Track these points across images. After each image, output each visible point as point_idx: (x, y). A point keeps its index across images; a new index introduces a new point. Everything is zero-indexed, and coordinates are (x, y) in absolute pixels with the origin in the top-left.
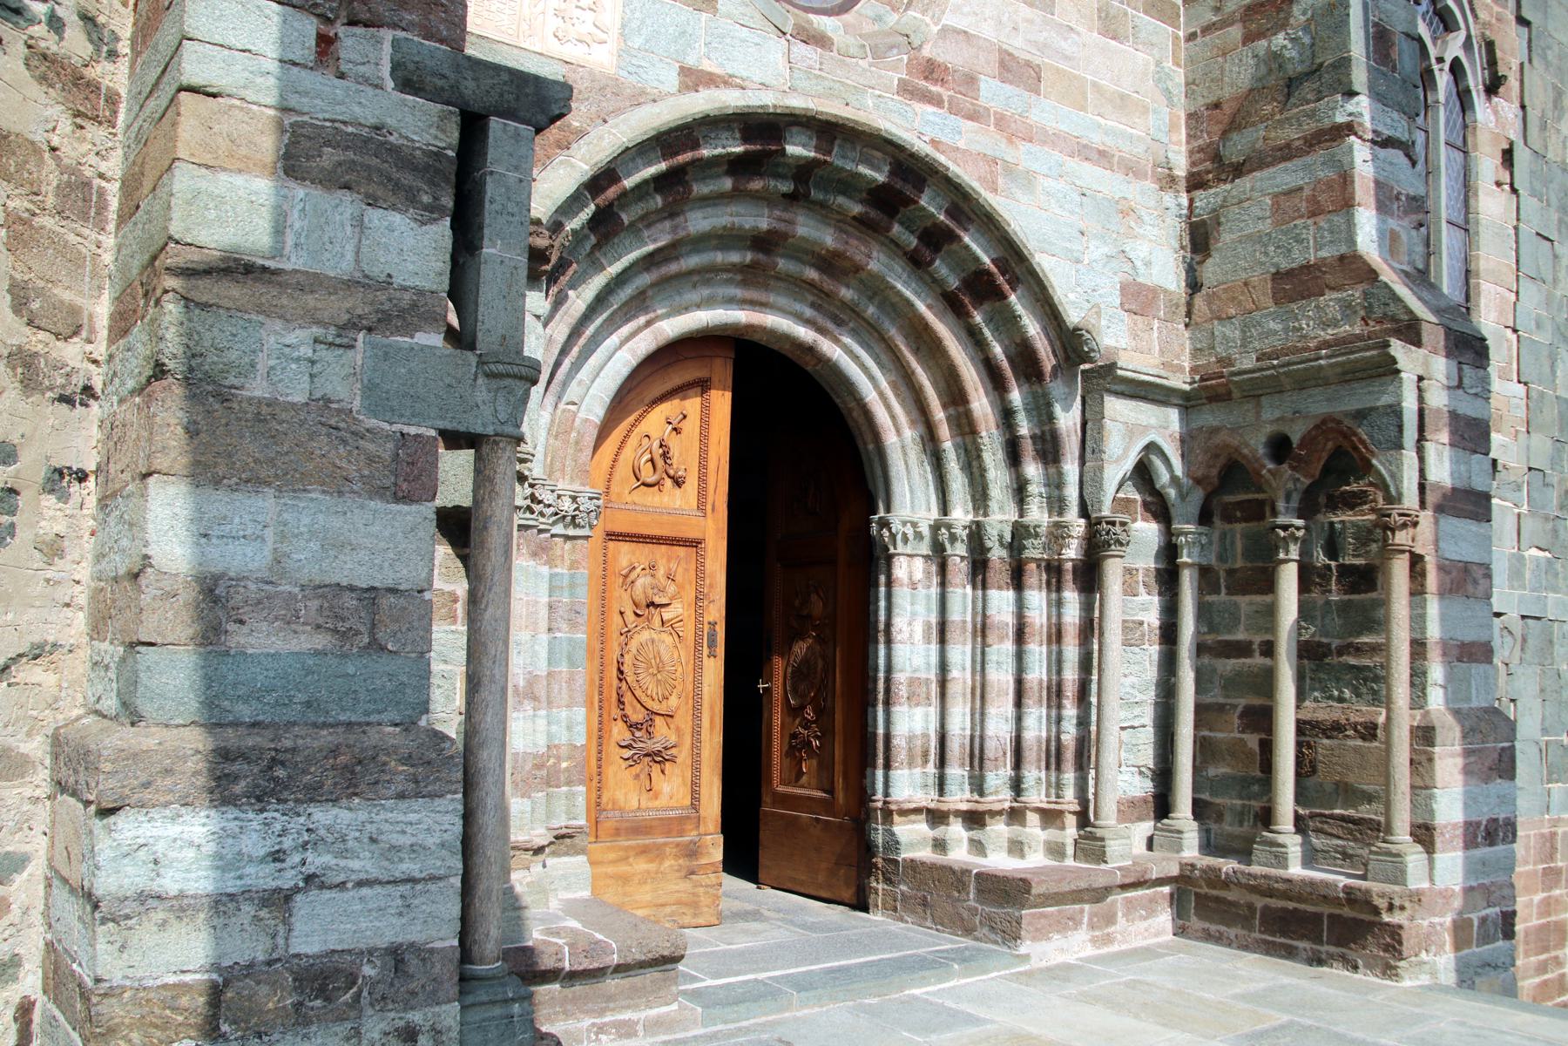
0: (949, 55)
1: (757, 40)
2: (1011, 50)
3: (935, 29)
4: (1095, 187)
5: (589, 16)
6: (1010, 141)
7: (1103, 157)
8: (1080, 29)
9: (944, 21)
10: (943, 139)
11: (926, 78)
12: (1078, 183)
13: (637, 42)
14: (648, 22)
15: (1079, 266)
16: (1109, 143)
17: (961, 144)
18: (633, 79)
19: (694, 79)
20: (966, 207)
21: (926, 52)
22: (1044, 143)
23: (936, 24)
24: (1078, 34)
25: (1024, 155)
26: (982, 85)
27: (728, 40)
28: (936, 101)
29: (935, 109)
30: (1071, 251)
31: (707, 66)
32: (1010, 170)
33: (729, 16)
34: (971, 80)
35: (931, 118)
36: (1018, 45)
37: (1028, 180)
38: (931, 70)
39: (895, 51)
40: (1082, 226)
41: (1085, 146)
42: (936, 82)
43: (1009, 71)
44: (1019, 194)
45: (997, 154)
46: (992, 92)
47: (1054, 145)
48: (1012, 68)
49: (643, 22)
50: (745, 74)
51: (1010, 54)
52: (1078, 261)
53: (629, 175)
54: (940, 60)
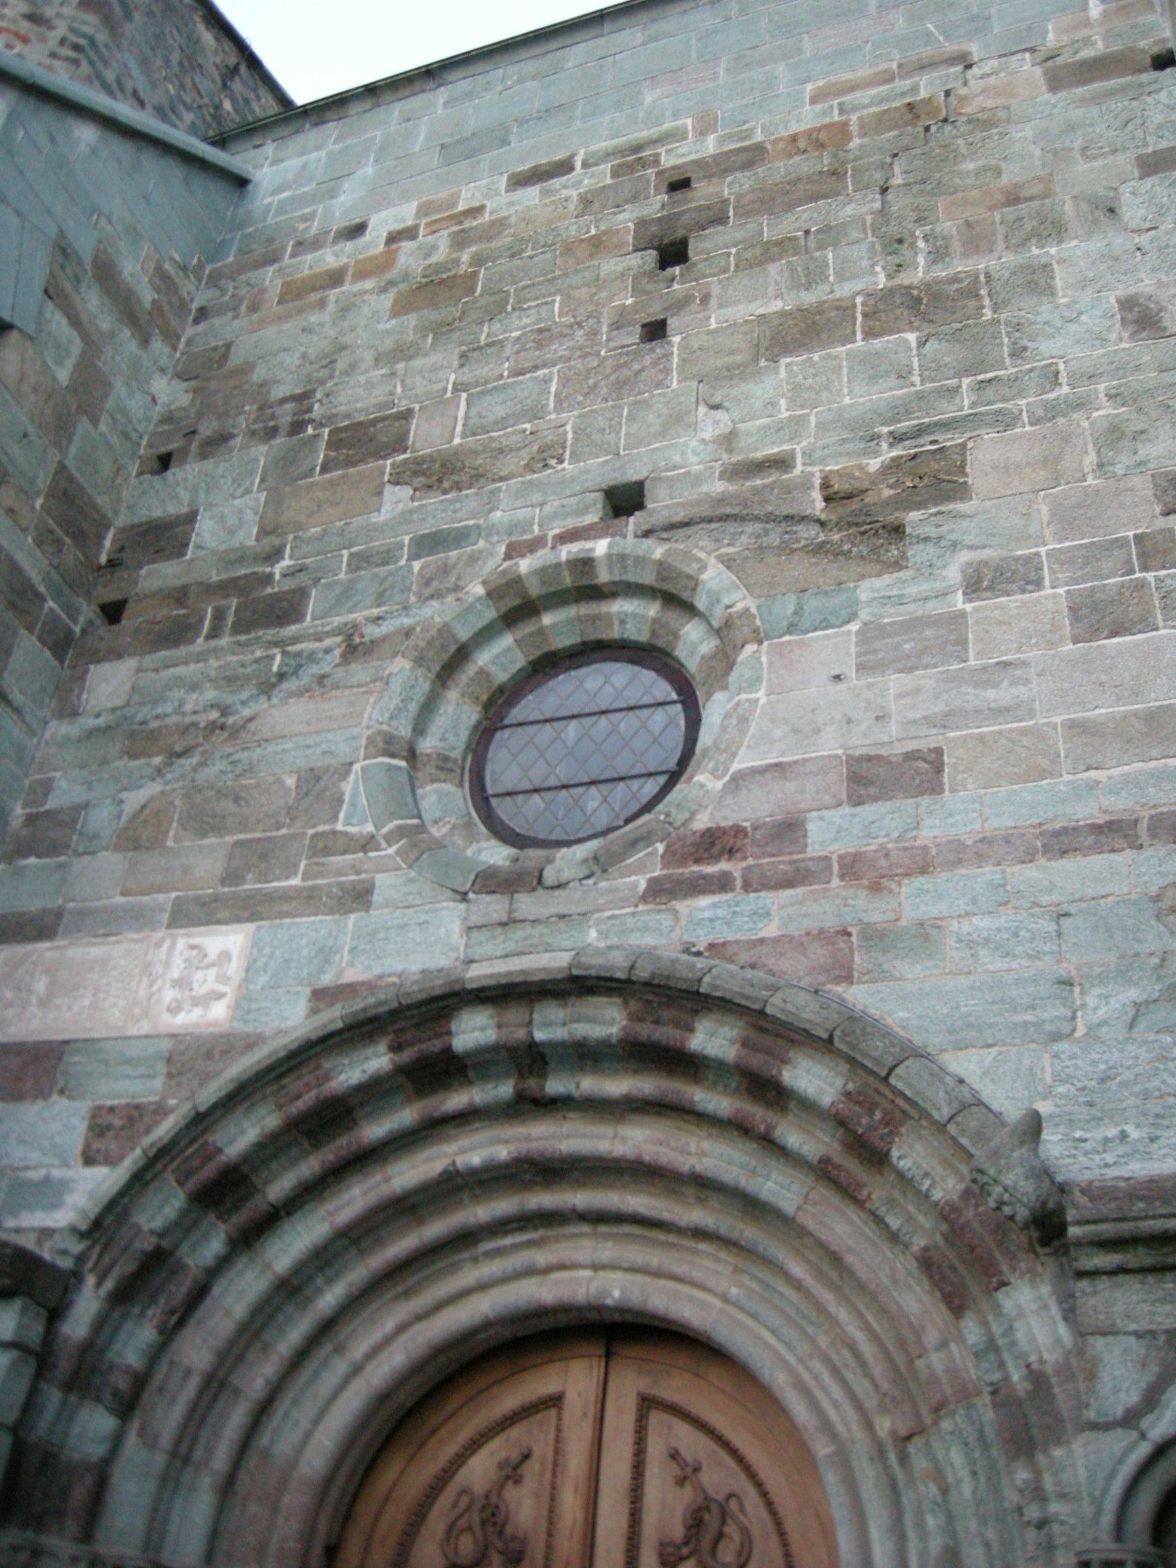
0: (753, 808)
1: (423, 917)
2: (873, 752)
3: (719, 785)
4: (1090, 892)
5: (212, 973)
6: (876, 888)
7: (1113, 833)
8: (1028, 655)
9: (732, 771)
10: (731, 937)
11: (697, 861)
12: (1045, 899)
13: (262, 980)
14: (278, 953)
15: (1064, 1046)
16: (1119, 804)
17: (770, 930)
18: (249, 1028)
19: (321, 996)
20: (770, 1030)
21: (702, 822)
22: (959, 862)
23: (718, 778)
24: (1025, 664)
25: (912, 901)
26: (812, 827)
27: (381, 935)
28: (723, 884)
29: (716, 898)
30: (1038, 1024)
31: (351, 976)
32: (878, 937)
33: (387, 904)
34: (789, 829)
35: (707, 914)
36: (893, 739)
37: (925, 936)
38: (717, 843)
39: (639, 846)
40: (1066, 969)
41: (1057, 834)
42: (716, 858)
43: (870, 783)
44: (903, 967)
45: (848, 918)
46: (830, 831)
47: (980, 859)
48: (865, 778)
49: (271, 956)
50: (399, 967)
51: (869, 759)
52: (1056, 1037)
53: (231, 1142)
54: (724, 824)
